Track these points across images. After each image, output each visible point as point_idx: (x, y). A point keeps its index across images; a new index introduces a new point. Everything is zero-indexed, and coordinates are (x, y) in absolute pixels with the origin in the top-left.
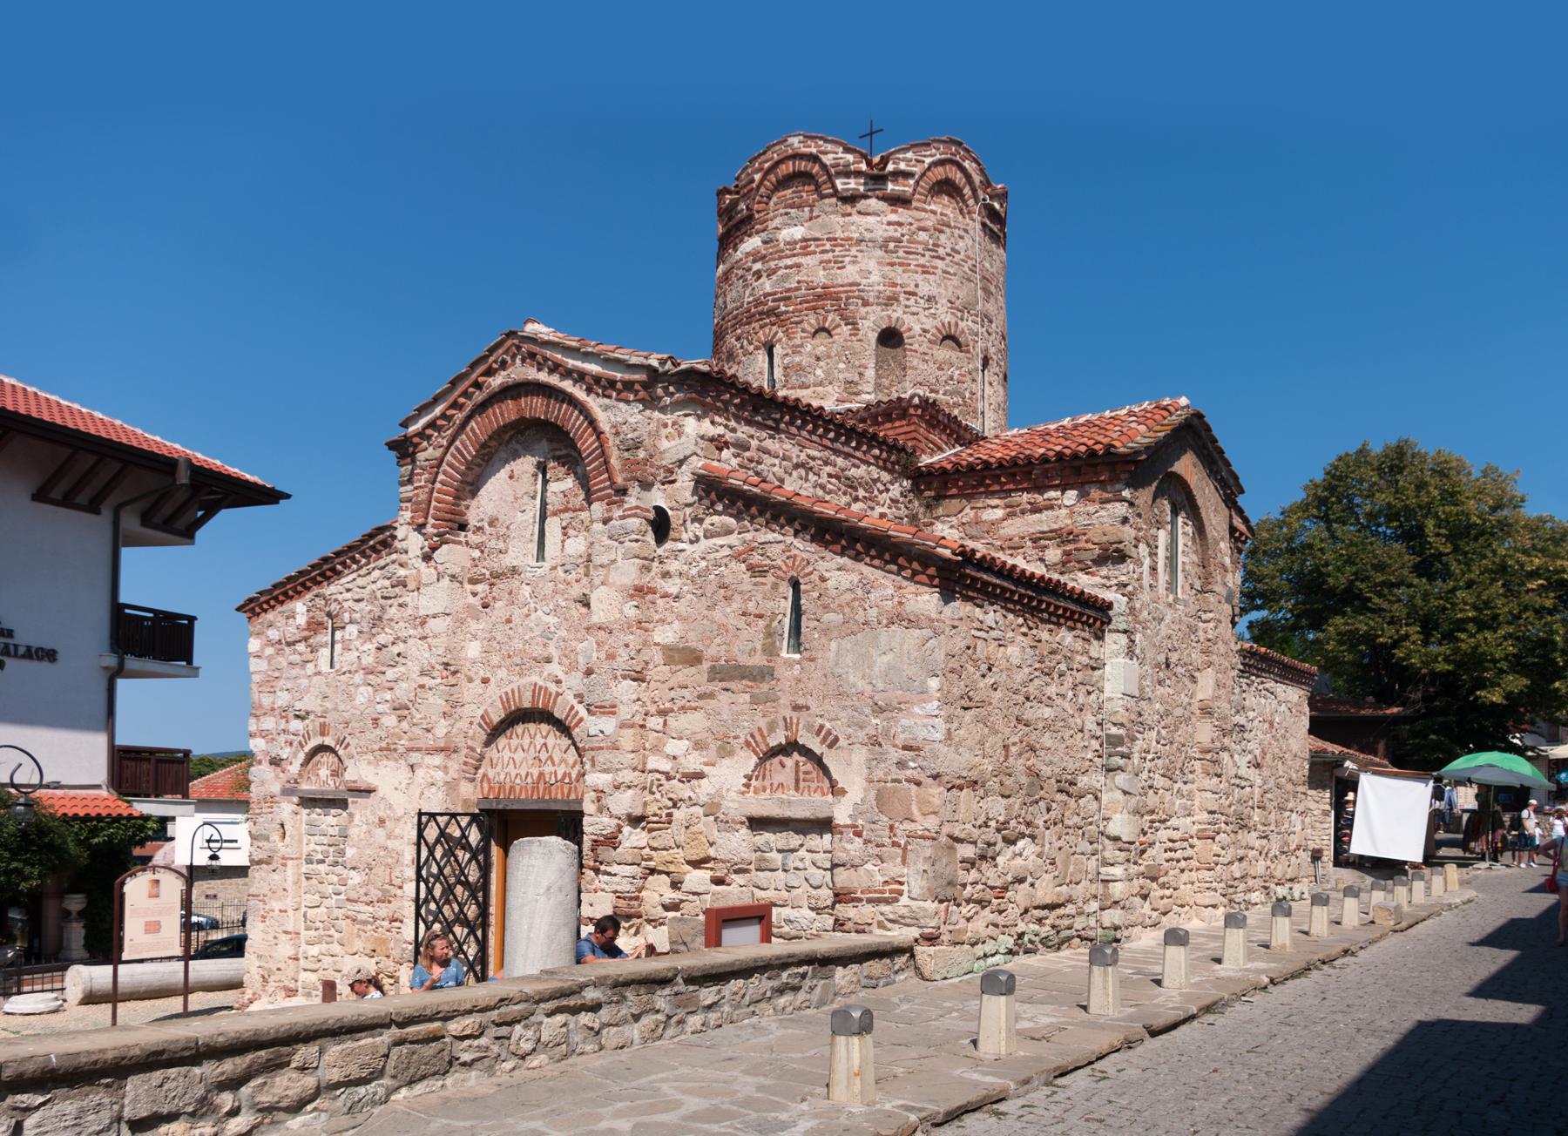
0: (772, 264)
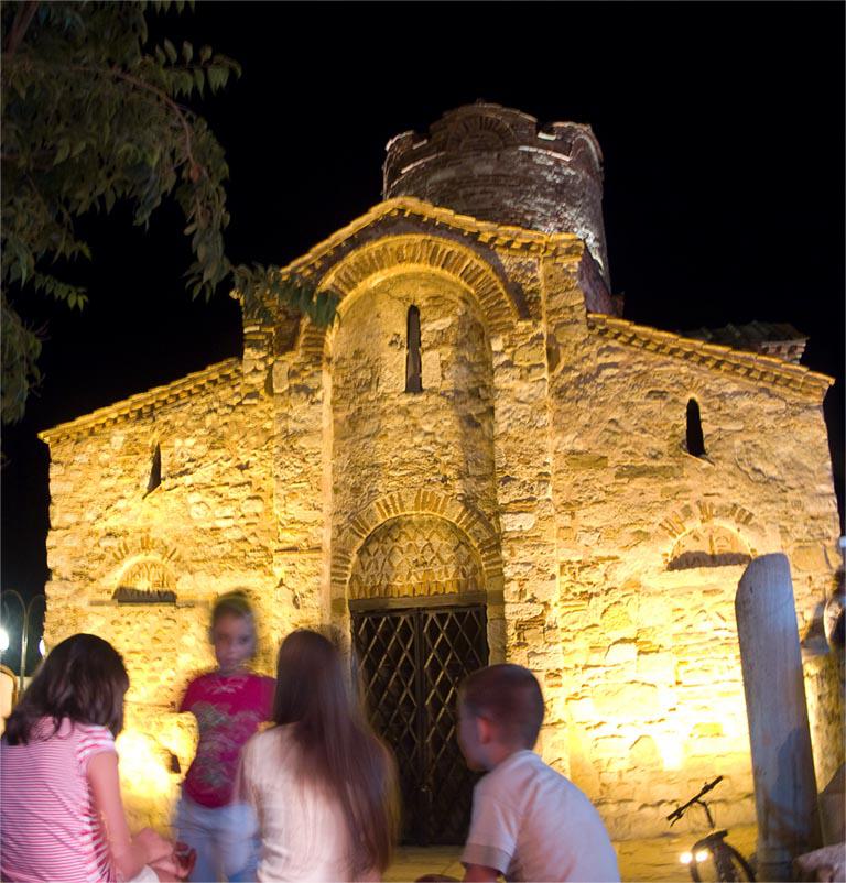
0: (469, 190)
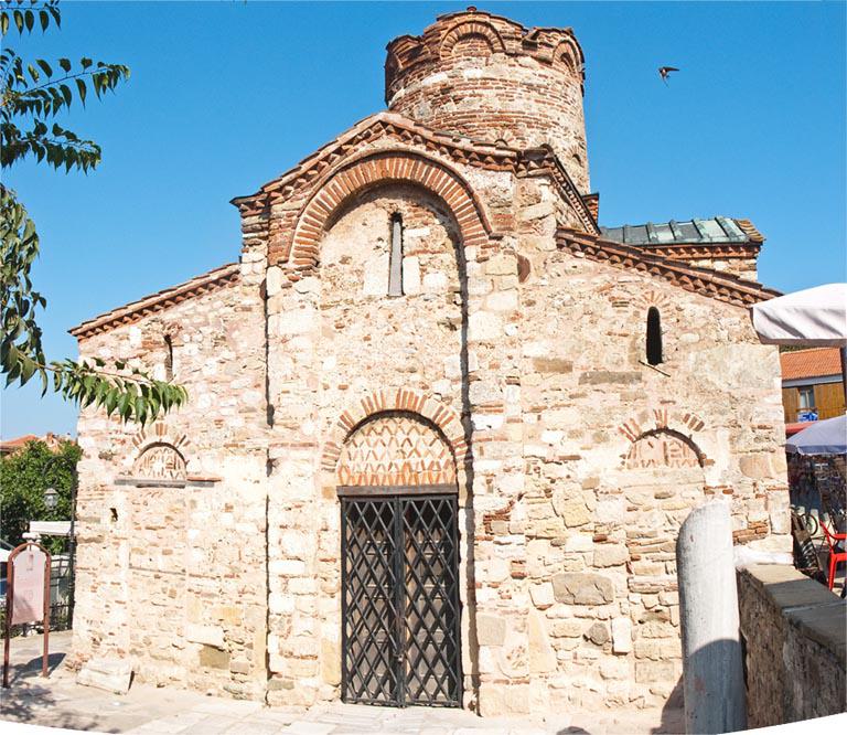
0: (459, 93)
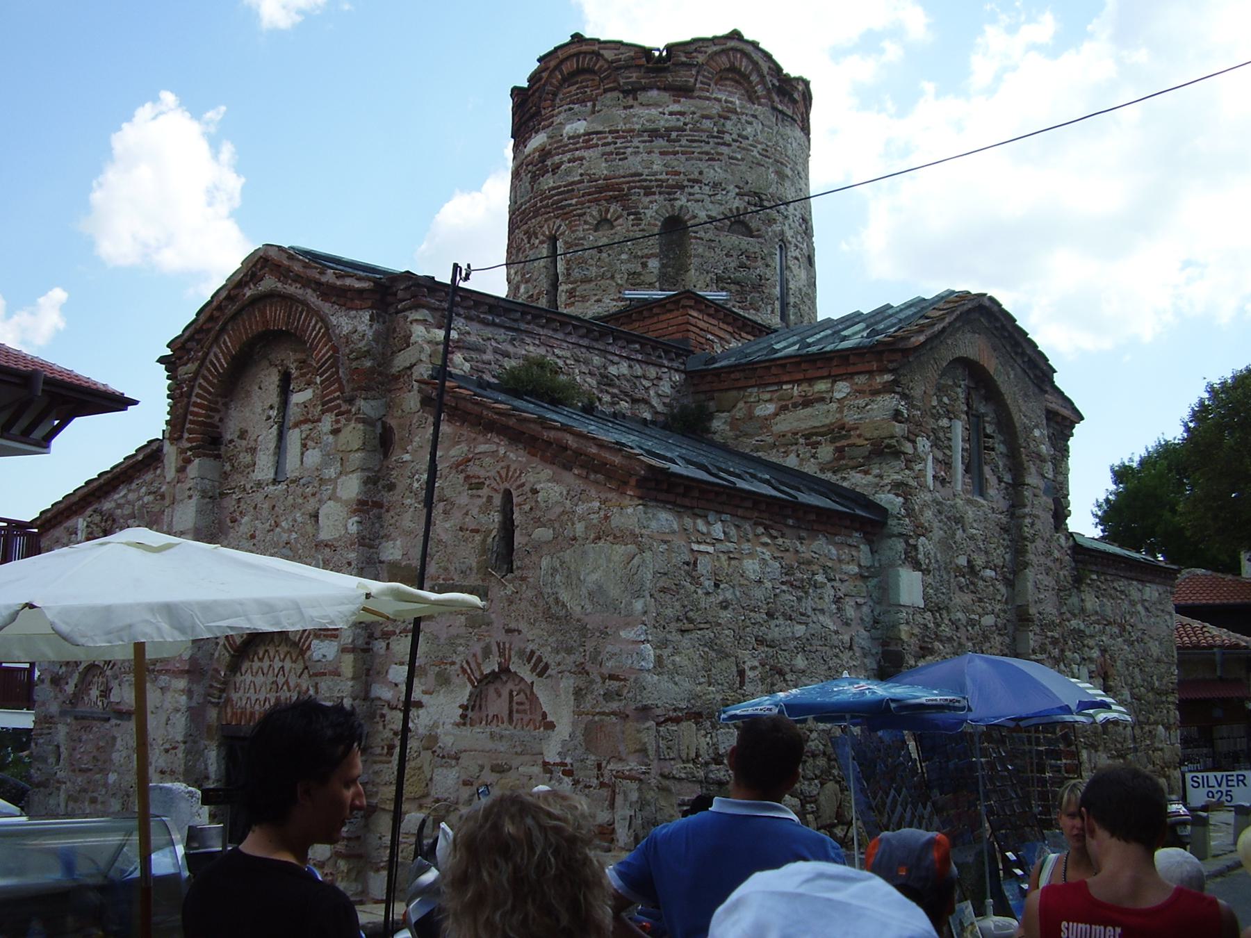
0: (557, 159)
